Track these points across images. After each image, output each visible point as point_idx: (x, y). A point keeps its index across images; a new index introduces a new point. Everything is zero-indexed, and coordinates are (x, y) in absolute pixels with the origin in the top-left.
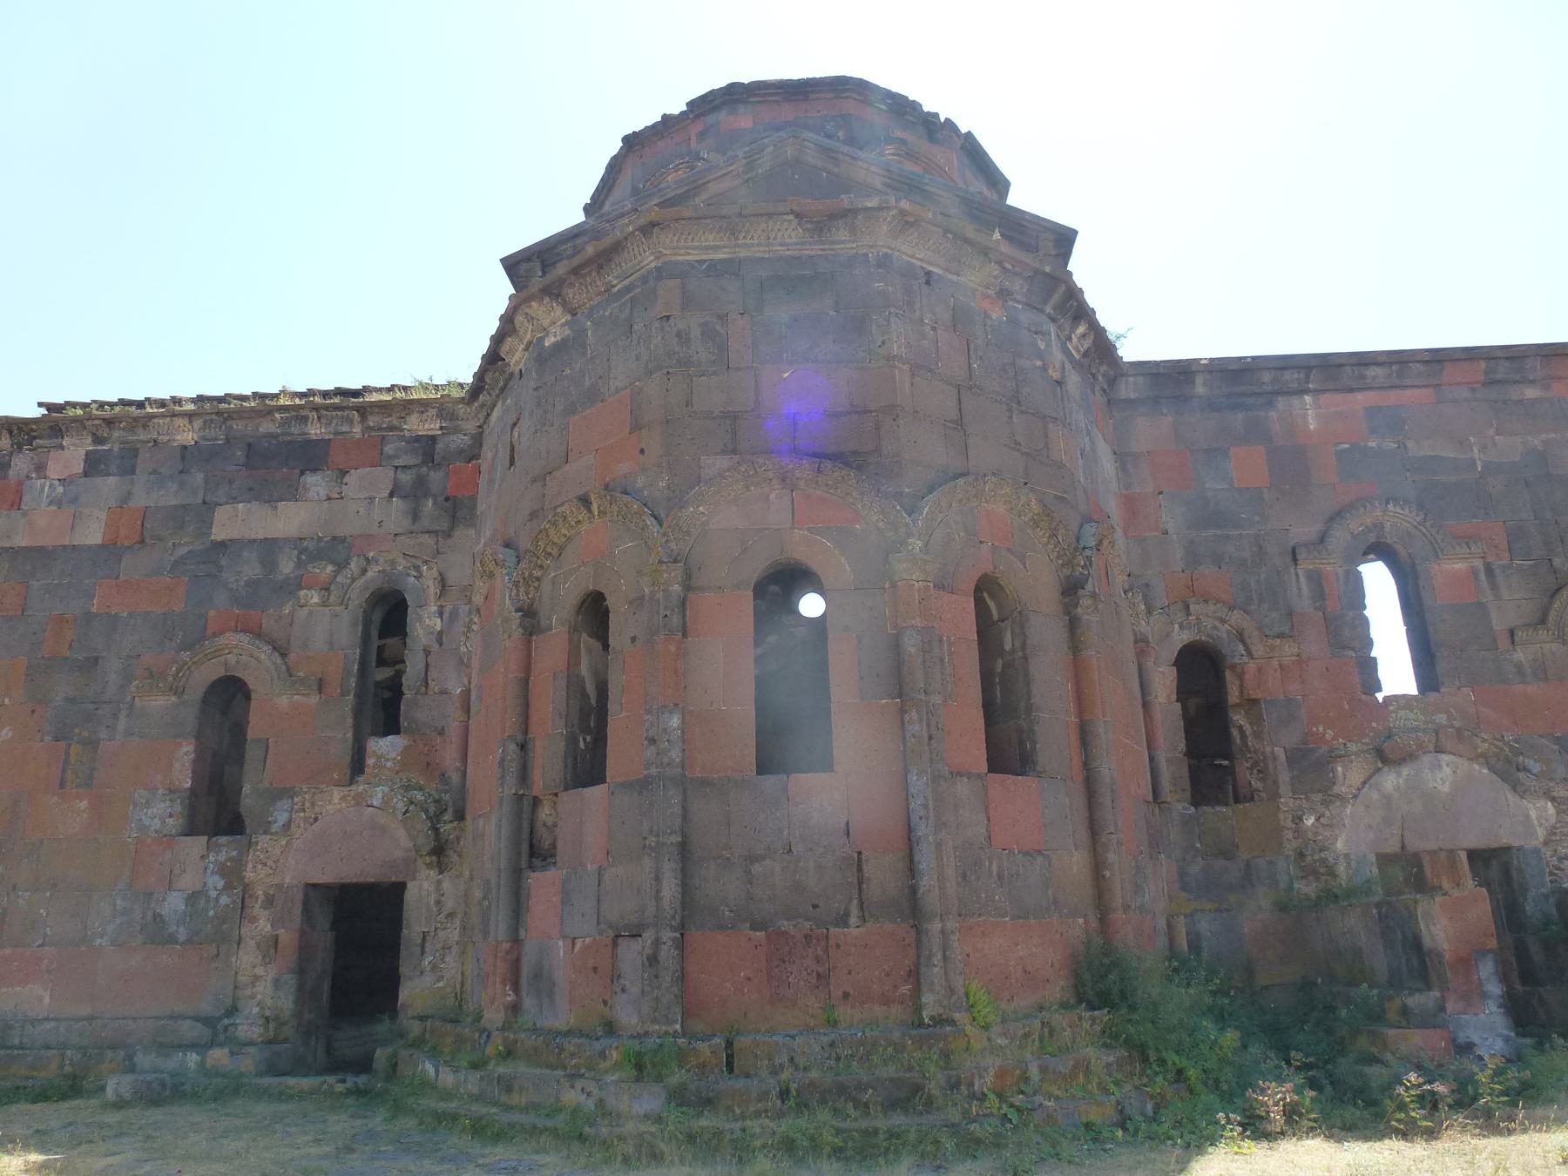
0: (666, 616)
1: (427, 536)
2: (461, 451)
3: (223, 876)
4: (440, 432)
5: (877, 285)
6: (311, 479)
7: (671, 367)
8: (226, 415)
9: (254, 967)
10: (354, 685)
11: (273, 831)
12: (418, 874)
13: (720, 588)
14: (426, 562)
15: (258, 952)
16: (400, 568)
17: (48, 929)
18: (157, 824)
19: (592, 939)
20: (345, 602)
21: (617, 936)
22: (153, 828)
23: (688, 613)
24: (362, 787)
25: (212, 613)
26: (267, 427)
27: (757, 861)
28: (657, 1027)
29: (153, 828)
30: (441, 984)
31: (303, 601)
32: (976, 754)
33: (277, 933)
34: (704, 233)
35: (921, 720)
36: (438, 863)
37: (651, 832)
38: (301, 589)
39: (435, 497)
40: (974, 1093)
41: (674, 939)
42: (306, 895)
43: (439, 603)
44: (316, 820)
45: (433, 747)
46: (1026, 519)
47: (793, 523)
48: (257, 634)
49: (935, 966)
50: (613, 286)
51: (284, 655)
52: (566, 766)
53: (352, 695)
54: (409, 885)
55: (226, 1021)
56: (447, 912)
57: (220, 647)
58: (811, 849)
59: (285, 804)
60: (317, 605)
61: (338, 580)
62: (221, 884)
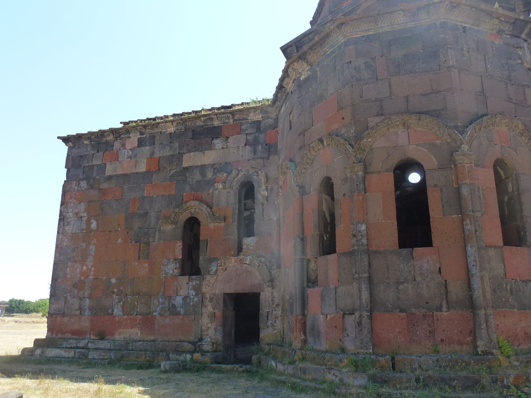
0: (357, 185)
1: (260, 159)
2: (270, 126)
3: (195, 290)
4: (262, 119)
5: (441, 36)
6: (216, 141)
7: (353, 82)
8: (184, 120)
11: (211, 273)
13: (379, 172)
14: (260, 170)
15: (208, 319)
16: (251, 173)
18: (171, 272)
19: (334, 315)
20: (231, 187)
21: (344, 314)
22: (170, 273)
23: (366, 183)
25: (185, 194)
26: (199, 123)
27: (401, 284)
28: (362, 351)
29: (170, 273)
30: (275, 332)
31: (216, 188)
32: (498, 238)
34: (363, 24)
35: (471, 224)
37: (356, 272)
38: (216, 183)
40: (504, 385)
41: (368, 316)
43: (266, 185)
44: (226, 269)
46: (517, 133)
47: (409, 143)
48: (201, 201)
49: (483, 329)
50: (327, 52)
51: (211, 208)
52: (320, 246)
54: (261, 294)
55: (199, 343)
58: (424, 279)
59: (214, 264)
60: (221, 189)
61: (228, 179)
62: (194, 294)
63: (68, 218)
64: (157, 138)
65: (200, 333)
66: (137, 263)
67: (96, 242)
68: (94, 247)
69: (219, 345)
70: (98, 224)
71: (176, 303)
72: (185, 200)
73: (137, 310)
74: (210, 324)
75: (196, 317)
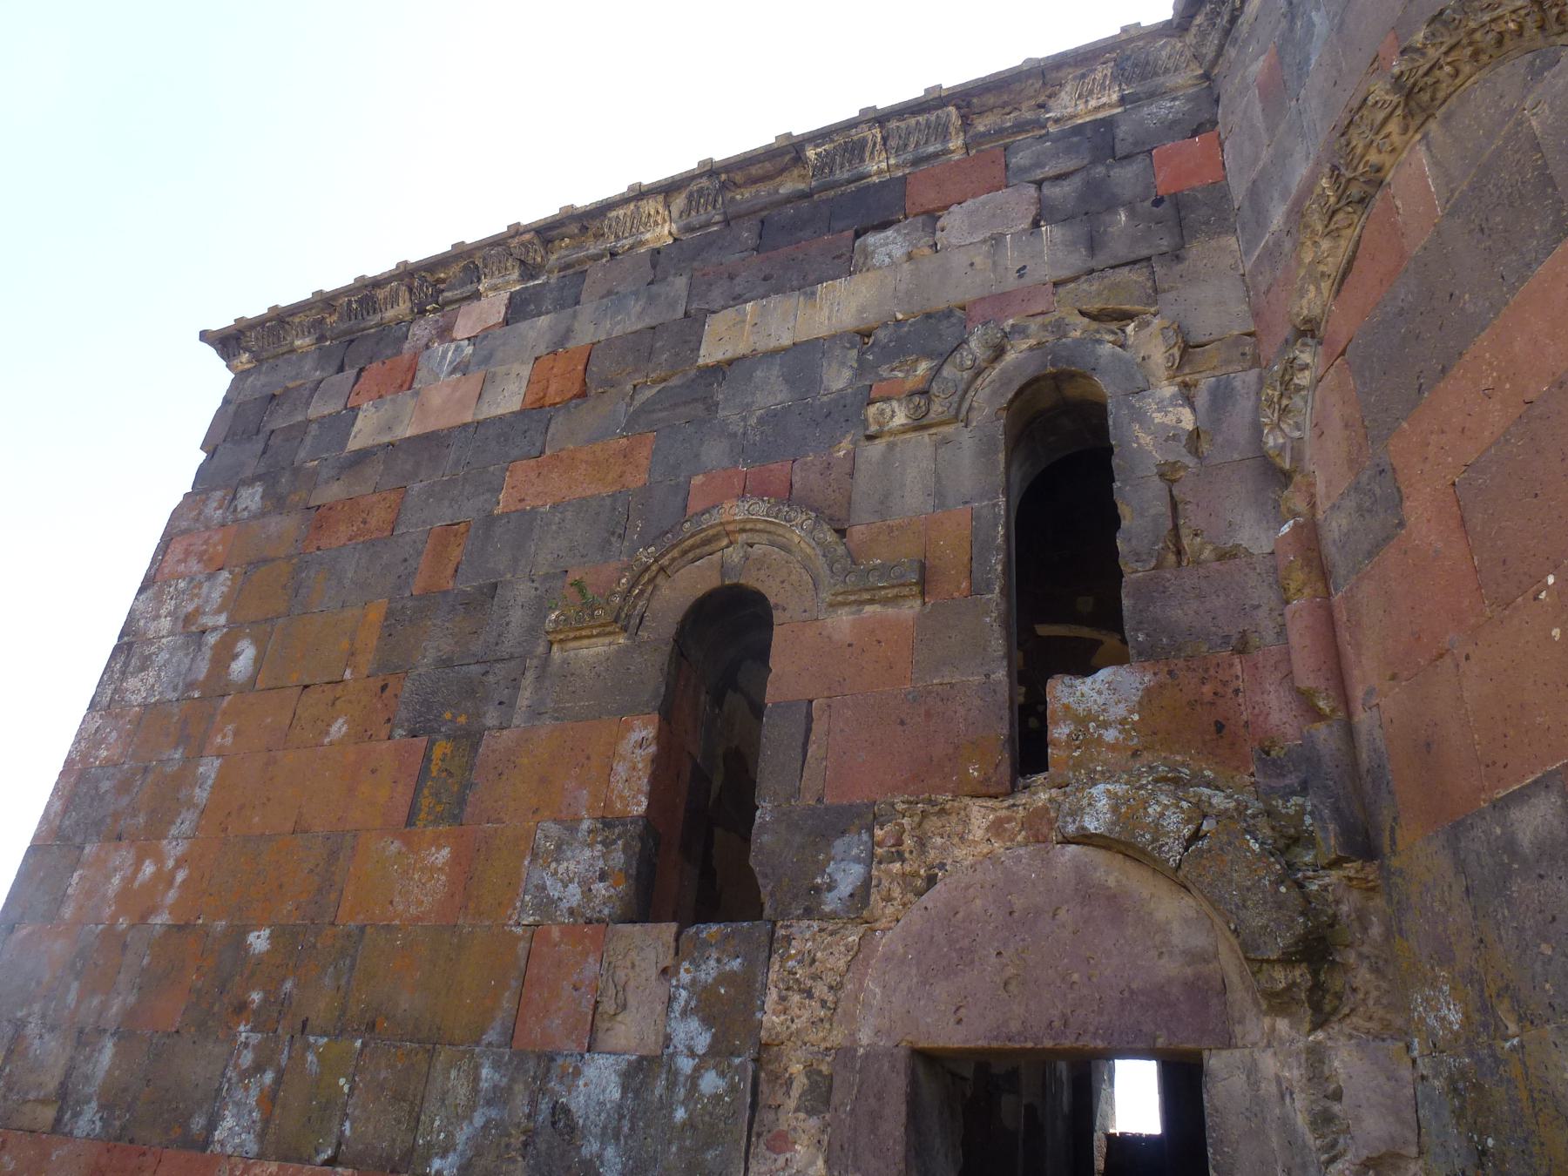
1: (1127, 268)
3: (707, 1021)
4: (1119, 110)
10: (999, 568)
11: (827, 909)
12: (1238, 1029)
17: (347, 1124)
18: (573, 895)
20: (962, 415)
22: (564, 905)
24: (1044, 796)
29: (564, 905)
36: (1311, 990)
38: (872, 402)
39: (1130, 207)
42: (914, 1083)
43: (1179, 379)
44: (931, 880)
45: (1225, 684)
48: (788, 496)
51: (841, 533)
53: (997, 590)
56: (1365, 1153)
57: (711, 532)
59: (851, 845)
60: (905, 430)
62: (703, 1042)
63: (150, 642)
64: (596, 273)
66: (396, 846)
67: (229, 740)
68: (217, 763)
70: (258, 661)
71: (577, 1102)
72: (695, 505)
73: (342, 1132)
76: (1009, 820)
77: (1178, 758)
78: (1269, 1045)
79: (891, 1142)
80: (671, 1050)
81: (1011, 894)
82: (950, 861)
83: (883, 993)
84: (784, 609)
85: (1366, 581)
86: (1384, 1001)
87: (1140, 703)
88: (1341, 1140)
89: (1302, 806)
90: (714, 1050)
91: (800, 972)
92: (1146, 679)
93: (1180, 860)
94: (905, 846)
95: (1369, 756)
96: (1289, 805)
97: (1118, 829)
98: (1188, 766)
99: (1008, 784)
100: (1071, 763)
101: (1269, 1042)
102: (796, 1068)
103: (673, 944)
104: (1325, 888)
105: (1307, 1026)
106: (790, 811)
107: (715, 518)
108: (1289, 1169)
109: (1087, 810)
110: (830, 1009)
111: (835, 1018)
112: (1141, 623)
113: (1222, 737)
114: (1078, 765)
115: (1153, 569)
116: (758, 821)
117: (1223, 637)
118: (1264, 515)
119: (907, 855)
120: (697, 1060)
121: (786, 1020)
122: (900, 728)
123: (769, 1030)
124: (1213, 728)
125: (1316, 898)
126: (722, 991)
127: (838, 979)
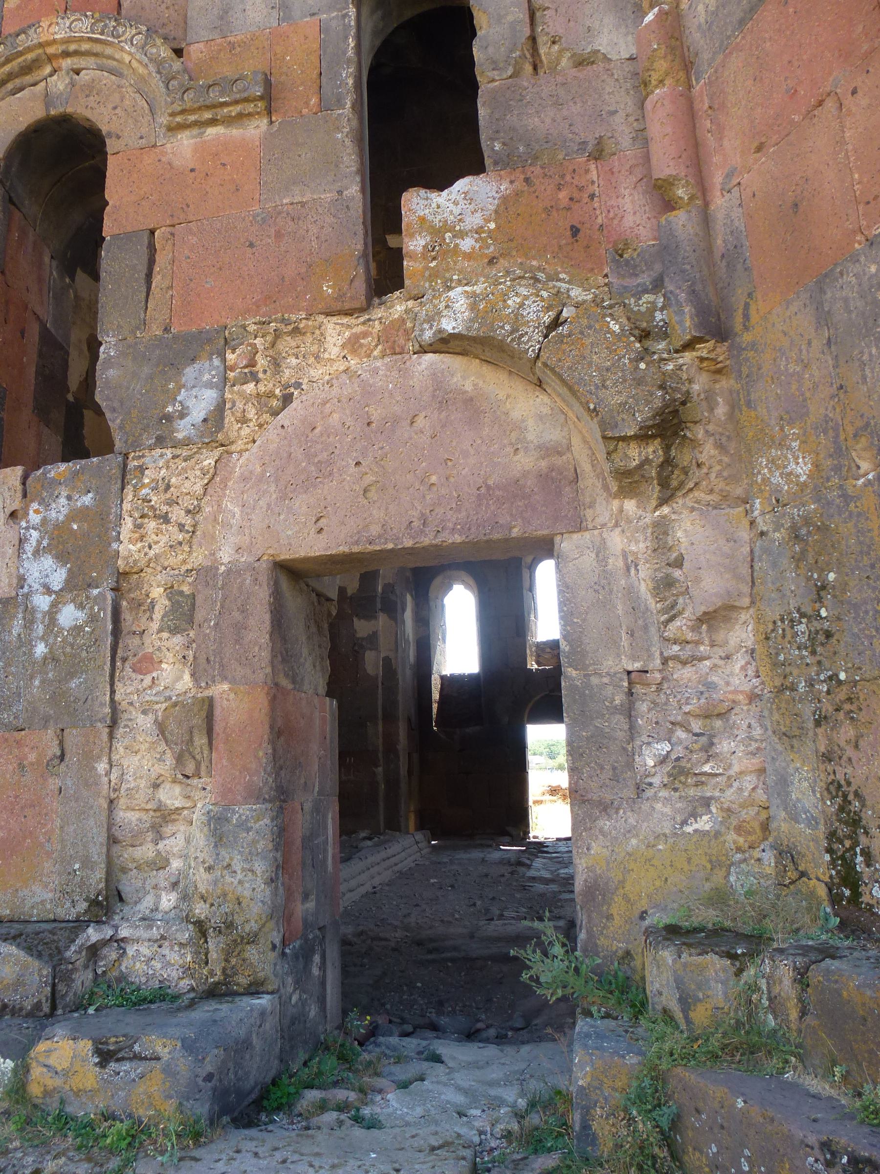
3: (61, 558)
9: (156, 786)
10: (350, 81)
11: (180, 436)
12: (589, 513)
15: (163, 746)
30: (704, 823)
33: (208, 693)
36: (661, 466)
42: (277, 593)
44: (287, 399)
45: (581, 189)
53: (349, 105)
55: (93, 935)
57: (30, 56)
62: (58, 578)
65: (97, 853)
69: (252, 939)
74: (177, 789)
75: (73, 737)
76: (365, 335)
77: (534, 263)
78: (616, 525)
79: (257, 649)
80: (26, 589)
81: (367, 406)
82: (306, 380)
83: (242, 512)
84: (118, 137)
85: (734, 55)
86: (725, 474)
87: (496, 212)
88: (681, 600)
89: (653, 303)
90: (70, 585)
91: (154, 499)
92: (502, 188)
93: (540, 349)
94: (259, 365)
95: (724, 241)
96: (641, 302)
97: (476, 325)
98: (544, 271)
99: (363, 298)
100: (427, 274)
101: (617, 522)
102: (157, 592)
103: (19, 487)
104: (680, 367)
105: (654, 503)
106: (136, 344)
107: (33, 38)
108: (632, 631)
109: (445, 313)
110: (188, 532)
111: (195, 540)
112: (497, 132)
113: (577, 241)
114: (434, 275)
115: (510, 77)
116: (102, 356)
117: (579, 144)
118: (623, 20)
119: (261, 375)
120: (54, 596)
121: (144, 547)
122: (249, 250)
123: (126, 558)
124: (569, 233)
125: (671, 378)
126: (75, 527)
127: (196, 503)
